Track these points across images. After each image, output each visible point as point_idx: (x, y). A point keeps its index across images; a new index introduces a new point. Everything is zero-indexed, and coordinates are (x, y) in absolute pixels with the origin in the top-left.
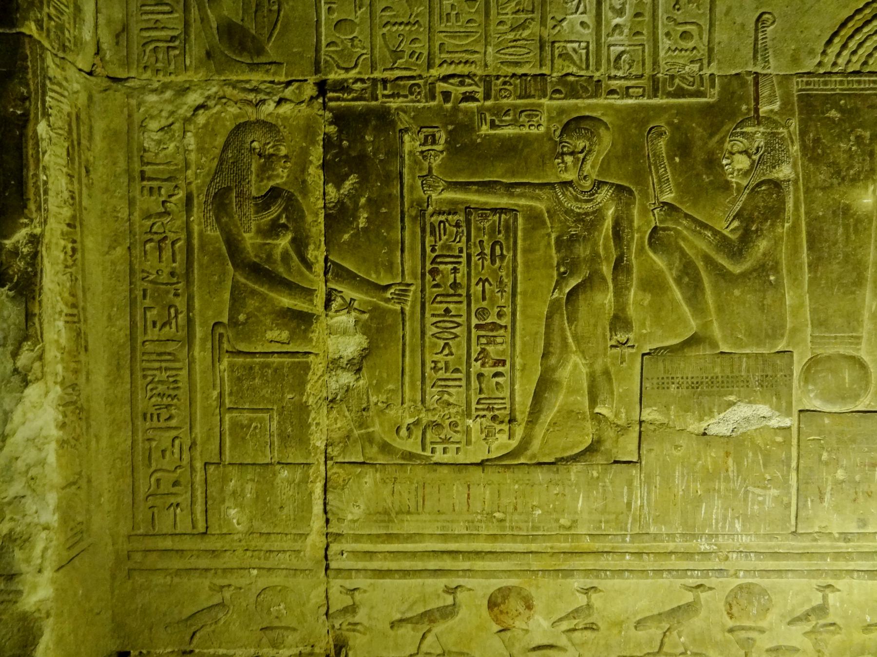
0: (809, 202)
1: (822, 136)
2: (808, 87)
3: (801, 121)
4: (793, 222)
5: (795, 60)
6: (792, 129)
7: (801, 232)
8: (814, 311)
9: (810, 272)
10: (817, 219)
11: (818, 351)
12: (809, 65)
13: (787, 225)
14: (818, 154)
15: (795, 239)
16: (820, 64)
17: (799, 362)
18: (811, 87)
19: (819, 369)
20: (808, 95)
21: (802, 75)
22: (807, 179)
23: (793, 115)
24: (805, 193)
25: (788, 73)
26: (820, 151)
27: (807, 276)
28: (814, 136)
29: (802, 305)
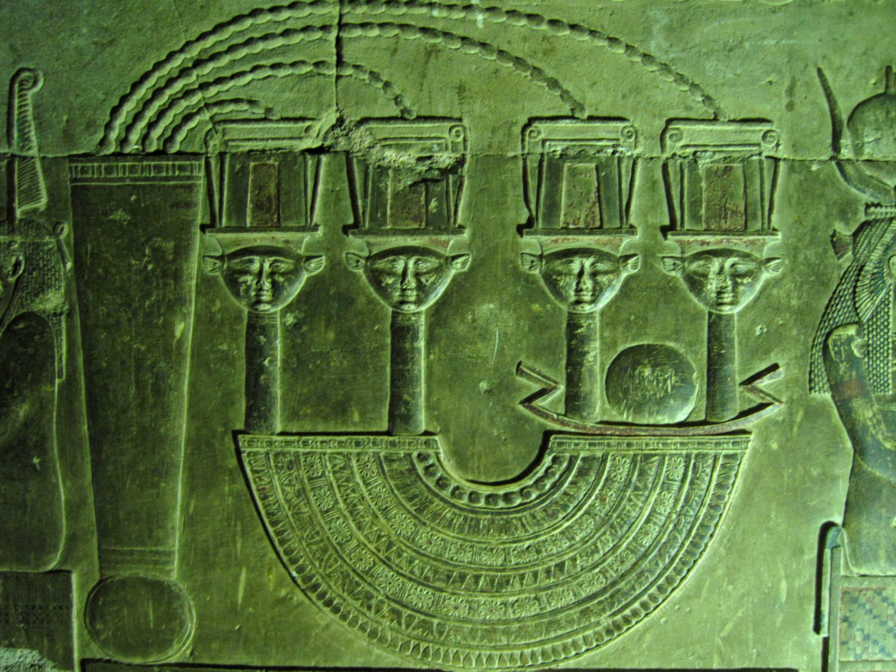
0: (89, 347)
1: (104, 249)
2: (85, 176)
3: (75, 227)
4: (68, 376)
5: (68, 137)
6: (62, 237)
7: (79, 389)
8: (100, 513)
9: (91, 453)
10: (99, 371)
11: (108, 573)
12: (88, 143)
13: (57, 381)
14: (99, 276)
15: (71, 402)
16: (103, 142)
17: (82, 586)
18: (89, 175)
19: (108, 599)
20: (84, 187)
21: (72, 158)
22: (84, 313)
23: (65, 217)
24: (82, 331)
25: (59, 155)
26: (100, 271)
27: (88, 458)
28: (92, 249)
29: (83, 502)
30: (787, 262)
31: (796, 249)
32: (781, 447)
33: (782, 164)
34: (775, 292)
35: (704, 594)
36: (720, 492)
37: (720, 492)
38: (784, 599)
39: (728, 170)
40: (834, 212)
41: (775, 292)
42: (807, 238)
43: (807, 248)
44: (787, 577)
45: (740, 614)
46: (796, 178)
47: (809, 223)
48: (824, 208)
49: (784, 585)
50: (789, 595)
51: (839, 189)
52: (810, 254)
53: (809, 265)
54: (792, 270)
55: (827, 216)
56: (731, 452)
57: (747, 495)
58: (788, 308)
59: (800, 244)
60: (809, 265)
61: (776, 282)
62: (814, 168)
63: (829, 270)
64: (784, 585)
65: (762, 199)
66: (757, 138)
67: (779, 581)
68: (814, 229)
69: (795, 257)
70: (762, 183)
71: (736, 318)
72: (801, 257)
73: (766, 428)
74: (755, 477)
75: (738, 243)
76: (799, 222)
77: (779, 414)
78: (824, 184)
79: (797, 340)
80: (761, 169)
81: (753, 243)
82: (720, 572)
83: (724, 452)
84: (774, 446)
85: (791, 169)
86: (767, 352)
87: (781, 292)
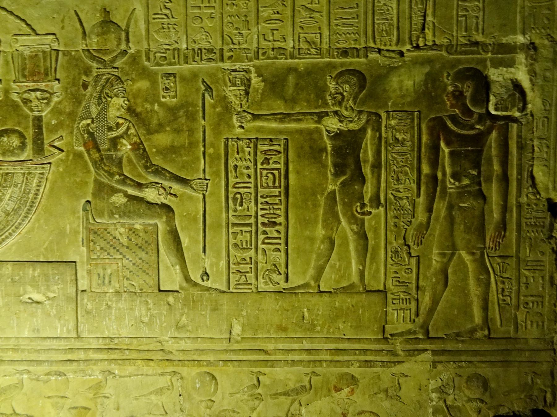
30: (63, 93)
31: (67, 88)
32: (64, 170)
33: (60, 53)
34: (59, 106)
35: (36, 230)
36: (38, 188)
37: (38, 188)
38: (68, 232)
39: (36, 55)
40: (82, 72)
41: (59, 106)
42: (71, 83)
43: (71, 87)
44: (70, 224)
45: (51, 238)
46: (67, 58)
47: (71, 77)
48: (78, 70)
49: (68, 227)
50: (70, 231)
51: (84, 62)
52: (73, 89)
53: (72, 94)
54: (66, 97)
55: (79, 74)
56: (41, 172)
57: (52, 189)
58: (65, 112)
59: (68, 86)
60: (72, 94)
61: (60, 102)
62: (73, 53)
63: (81, 97)
64: (68, 227)
65: (51, 67)
66: (48, 42)
67: (66, 225)
68: (74, 79)
69: (67, 91)
70: (51, 60)
71: (44, 117)
72: (69, 91)
73: (58, 162)
74: (54, 182)
75: (42, 85)
76: (68, 77)
77: (63, 156)
78: (77, 60)
79: (68, 126)
80: (51, 55)
81: (47, 85)
82: (42, 221)
83: (39, 172)
84: (61, 169)
85: (64, 54)
86: (57, 131)
87: (62, 106)
